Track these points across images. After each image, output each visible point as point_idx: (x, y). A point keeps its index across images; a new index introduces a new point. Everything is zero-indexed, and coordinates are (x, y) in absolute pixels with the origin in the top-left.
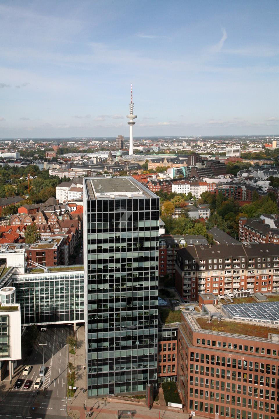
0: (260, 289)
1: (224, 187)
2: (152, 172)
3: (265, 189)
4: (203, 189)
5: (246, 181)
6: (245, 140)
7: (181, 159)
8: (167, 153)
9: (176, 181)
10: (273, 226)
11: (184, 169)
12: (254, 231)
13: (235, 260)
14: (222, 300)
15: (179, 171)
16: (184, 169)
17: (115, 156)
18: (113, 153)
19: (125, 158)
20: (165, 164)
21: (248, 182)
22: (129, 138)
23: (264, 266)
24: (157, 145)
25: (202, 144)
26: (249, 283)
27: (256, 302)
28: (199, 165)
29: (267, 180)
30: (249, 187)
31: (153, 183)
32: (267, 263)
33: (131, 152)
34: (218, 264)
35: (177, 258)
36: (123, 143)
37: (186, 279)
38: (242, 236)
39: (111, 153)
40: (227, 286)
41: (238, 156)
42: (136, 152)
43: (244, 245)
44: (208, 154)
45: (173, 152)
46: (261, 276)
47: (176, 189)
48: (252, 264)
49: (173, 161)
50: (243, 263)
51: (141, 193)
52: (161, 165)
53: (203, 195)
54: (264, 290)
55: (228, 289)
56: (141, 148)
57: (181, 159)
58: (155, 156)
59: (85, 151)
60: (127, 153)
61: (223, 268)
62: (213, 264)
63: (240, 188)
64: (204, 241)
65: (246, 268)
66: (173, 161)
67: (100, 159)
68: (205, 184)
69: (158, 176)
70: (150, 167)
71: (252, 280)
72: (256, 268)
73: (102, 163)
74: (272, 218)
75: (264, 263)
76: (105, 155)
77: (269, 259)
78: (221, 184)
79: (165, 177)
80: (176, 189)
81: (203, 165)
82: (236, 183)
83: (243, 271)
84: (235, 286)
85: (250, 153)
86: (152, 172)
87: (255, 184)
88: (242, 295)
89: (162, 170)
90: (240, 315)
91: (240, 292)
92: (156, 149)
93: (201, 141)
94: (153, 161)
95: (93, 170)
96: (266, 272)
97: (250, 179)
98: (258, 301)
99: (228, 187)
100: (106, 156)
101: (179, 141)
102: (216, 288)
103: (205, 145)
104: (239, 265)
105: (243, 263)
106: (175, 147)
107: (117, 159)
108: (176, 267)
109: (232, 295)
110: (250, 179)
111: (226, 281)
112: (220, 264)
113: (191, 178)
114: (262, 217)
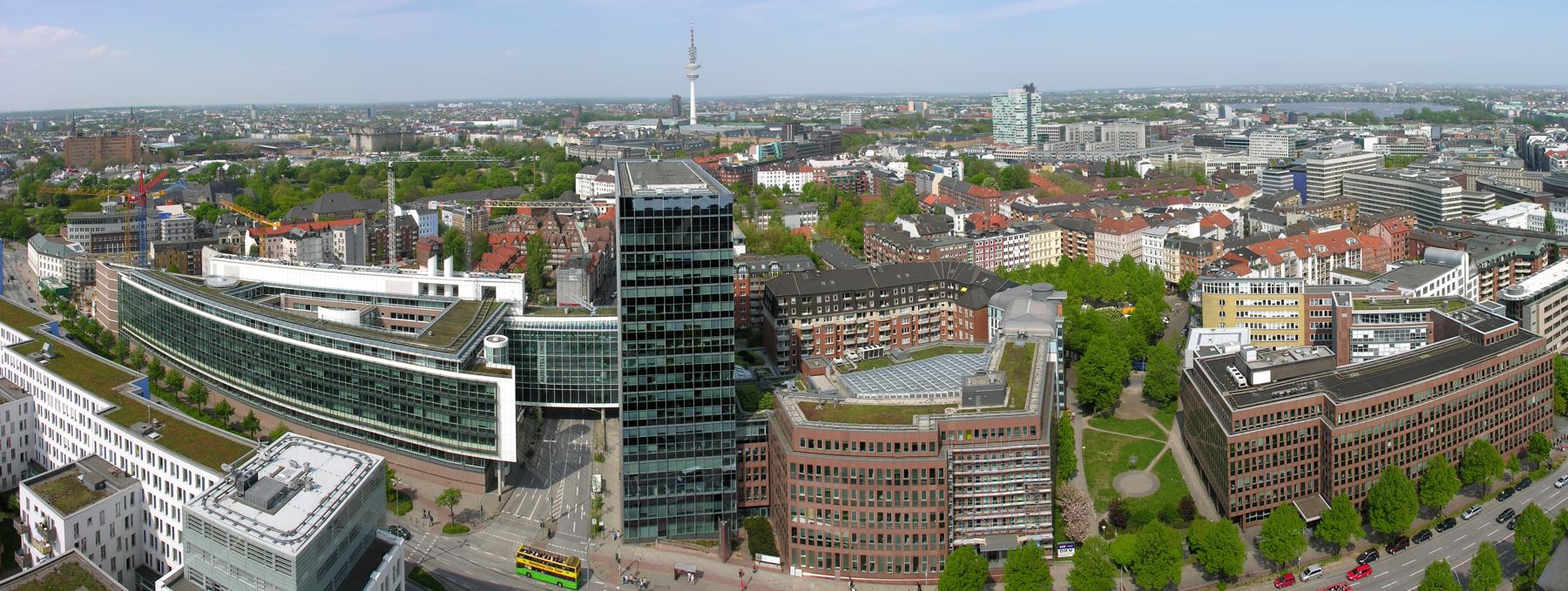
0: (900, 342)
1: (839, 174)
2: (726, 151)
3: (901, 176)
4: (808, 177)
5: (872, 163)
6: (869, 100)
7: (771, 129)
8: (749, 121)
9: (764, 165)
10: (915, 233)
11: (776, 146)
12: (887, 244)
13: (859, 295)
14: (839, 366)
15: (770, 150)
16: (776, 146)
17: (667, 127)
18: (665, 121)
19: (684, 130)
20: (747, 138)
21: (875, 164)
22: (689, 100)
23: (904, 301)
24: (733, 110)
25: (804, 106)
26: (882, 333)
27: (893, 364)
28: (799, 140)
29: (904, 160)
30: (877, 173)
31: (726, 169)
32: (907, 296)
33: (693, 122)
34: (832, 303)
35: (765, 296)
36: (678, 107)
37: (781, 333)
38: (869, 254)
39: (660, 122)
40: (847, 342)
41: (859, 125)
42: (700, 120)
43: (871, 268)
44: (814, 121)
45: (759, 119)
46: (900, 318)
47: (764, 178)
48: (886, 300)
49: (758, 133)
50: (871, 299)
51: (705, 185)
52: (739, 140)
53: (806, 187)
54: (906, 341)
55: (849, 346)
56: (708, 114)
57: (771, 129)
58: (732, 127)
59: (621, 119)
60: (688, 123)
61: (841, 310)
62: (823, 304)
63: (863, 173)
64: (809, 265)
65: (877, 307)
66: (758, 133)
67: (645, 131)
68: (810, 169)
69: (735, 158)
70: (722, 145)
71: (887, 328)
72: (892, 305)
73: (647, 138)
74: (912, 221)
75: (903, 296)
76: (652, 125)
77: (911, 289)
78: (835, 169)
79: (746, 159)
80: (764, 178)
81: (806, 138)
82: (858, 167)
83: (872, 314)
84: (862, 340)
85: (876, 120)
86: (726, 151)
87: (886, 168)
88: (871, 356)
89: (743, 148)
90: (869, 389)
91: (868, 349)
92: (733, 115)
93: (802, 101)
94: (727, 134)
95: (633, 148)
96: (908, 311)
97: (878, 159)
98: (896, 361)
99: (845, 173)
100: (655, 127)
101: (769, 102)
102: (829, 348)
103: (809, 107)
104: (864, 303)
105: (871, 299)
106: (764, 110)
107: (669, 132)
108: (765, 312)
109: (856, 356)
110: (878, 159)
111: (846, 332)
112: (836, 303)
113: (787, 159)
114: (898, 220)
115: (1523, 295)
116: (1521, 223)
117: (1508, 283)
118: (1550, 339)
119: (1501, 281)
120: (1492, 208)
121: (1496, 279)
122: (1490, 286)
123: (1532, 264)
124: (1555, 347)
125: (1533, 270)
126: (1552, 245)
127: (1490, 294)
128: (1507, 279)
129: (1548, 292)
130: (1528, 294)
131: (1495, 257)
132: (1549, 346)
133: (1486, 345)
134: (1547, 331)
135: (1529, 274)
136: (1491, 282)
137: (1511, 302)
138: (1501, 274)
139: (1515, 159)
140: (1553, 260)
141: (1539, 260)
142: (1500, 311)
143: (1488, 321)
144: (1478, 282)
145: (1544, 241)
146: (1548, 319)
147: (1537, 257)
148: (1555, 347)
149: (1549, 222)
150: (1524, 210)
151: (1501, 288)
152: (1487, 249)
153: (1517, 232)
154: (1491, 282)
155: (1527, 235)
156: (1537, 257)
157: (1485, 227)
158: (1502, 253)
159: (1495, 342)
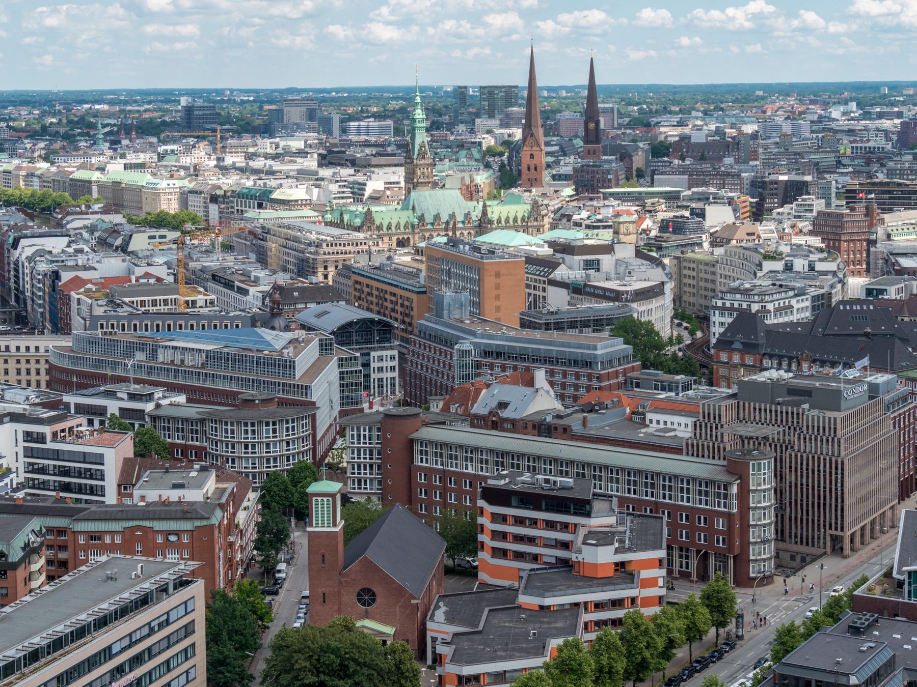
126: (61, 532)
141: (21, 573)
145: (36, 523)
147: (14, 566)
156: (14, 566)
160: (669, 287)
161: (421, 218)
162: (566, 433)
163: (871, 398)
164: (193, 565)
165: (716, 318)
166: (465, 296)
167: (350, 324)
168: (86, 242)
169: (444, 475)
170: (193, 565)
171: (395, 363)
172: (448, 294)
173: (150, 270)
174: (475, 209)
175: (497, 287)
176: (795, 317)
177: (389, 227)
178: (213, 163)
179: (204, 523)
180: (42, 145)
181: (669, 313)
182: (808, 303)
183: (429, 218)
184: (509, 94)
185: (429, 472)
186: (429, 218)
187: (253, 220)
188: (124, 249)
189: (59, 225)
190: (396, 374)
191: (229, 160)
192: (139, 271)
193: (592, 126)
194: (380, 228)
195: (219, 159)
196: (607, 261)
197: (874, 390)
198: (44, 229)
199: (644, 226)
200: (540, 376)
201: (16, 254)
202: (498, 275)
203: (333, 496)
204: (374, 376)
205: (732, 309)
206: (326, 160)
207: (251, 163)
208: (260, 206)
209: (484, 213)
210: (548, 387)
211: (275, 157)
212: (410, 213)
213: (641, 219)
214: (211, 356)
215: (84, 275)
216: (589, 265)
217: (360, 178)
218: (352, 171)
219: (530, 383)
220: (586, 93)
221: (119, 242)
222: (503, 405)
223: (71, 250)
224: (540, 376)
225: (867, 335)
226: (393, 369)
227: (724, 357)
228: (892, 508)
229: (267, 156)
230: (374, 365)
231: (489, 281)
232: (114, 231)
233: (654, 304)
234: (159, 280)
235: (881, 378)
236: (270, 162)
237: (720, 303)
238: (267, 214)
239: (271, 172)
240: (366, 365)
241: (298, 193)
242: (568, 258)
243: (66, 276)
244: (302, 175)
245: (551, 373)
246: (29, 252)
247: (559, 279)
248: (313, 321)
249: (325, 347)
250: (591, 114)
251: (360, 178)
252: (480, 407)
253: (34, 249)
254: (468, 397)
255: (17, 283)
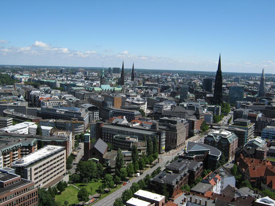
115: (24, 164)
116: (25, 131)
117: (17, 158)
118: (37, 182)
119: (14, 158)
120: (11, 125)
121: (12, 157)
122: (8, 160)
123: (28, 150)
124: (40, 185)
125: (31, 152)
127: (8, 164)
128: (17, 157)
129: (36, 162)
130: (26, 163)
131: (11, 147)
132: (36, 186)
133: (5, 187)
134: (35, 179)
135: (28, 154)
136: (9, 159)
137: (18, 167)
138: (14, 155)
139: (24, 102)
140: (39, 147)
142: (11, 171)
143: (6, 176)
144: (2, 159)
145: (35, 139)
146: (35, 174)
147: (32, 147)
148: (40, 185)
149: (39, 131)
150: (26, 125)
151: (14, 161)
152: (7, 144)
153: (23, 136)
154: (9, 159)
155: (29, 137)
157: (6, 134)
158: (14, 146)
159: (9, 185)
160: (146, 103)
161: (103, 90)
162: (128, 127)
163: (182, 122)
164: (64, 147)
165: (154, 108)
166: (111, 103)
167: (91, 107)
168: (43, 92)
169: (108, 134)
170: (64, 147)
171: (98, 114)
172: (108, 103)
173: (55, 97)
174: (112, 88)
175: (117, 102)
176: (168, 109)
177: (97, 91)
178: (66, 79)
179: (65, 140)
180: (35, 75)
181: (146, 107)
182: (170, 107)
183: (104, 90)
184: (118, 69)
185: (105, 133)
186: (104, 90)
187: (73, 89)
188: (50, 93)
189: (39, 88)
190: (98, 116)
191: (69, 79)
192: (53, 97)
193: (133, 75)
194: (96, 91)
195: (67, 78)
196: (135, 98)
197: (182, 121)
198: (36, 89)
199: (142, 93)
200: (124, 117)
201: (31, 93)
202: (117, 100)
203: (88, 136)
204: (94, 116)
205: (157, 107)
206: (86, 79)
207: (73, 79)
208: (74, 87)
209: (114, 89)
210: (126, 119)
211: (77, 78)
212: (101, 89)
213: (141, 92)
214: (66, 112)
215: (43, 97)
216: (132, 99)
217: (92, 82)
218: (90, 81)
219: (123, 118)
220: (132, 70)
221: (49, 92)
222: (118, 122)
223: (41, 93)
224: (124, 117)
225: (181, 112)
226: (98, 115)
227: (156, 115)
228: (184, 141)
229: (75, 78)
230: (95, 115)
231: (115, 101)
232: (48, 90)
233: (144, 106)
234: (57, 98)
235: (183, 119)
236: (76, 79)
237: (155, 106)
238: (75, 88)
239: (76, 81)
240: (93, 115)
241: (81, 85)
242: (129, 97)
243: (40, 97)
244: (82, 82)
245: (126, 118)
246: (33, 93)
247: (127, 101)
248: (84, 106)
249: (86, 111)
250: (133, 73)
251: (92, 82)
252: (114, 122)
253: (34, 93)
254: (111, 120)
255: (31, 98)
